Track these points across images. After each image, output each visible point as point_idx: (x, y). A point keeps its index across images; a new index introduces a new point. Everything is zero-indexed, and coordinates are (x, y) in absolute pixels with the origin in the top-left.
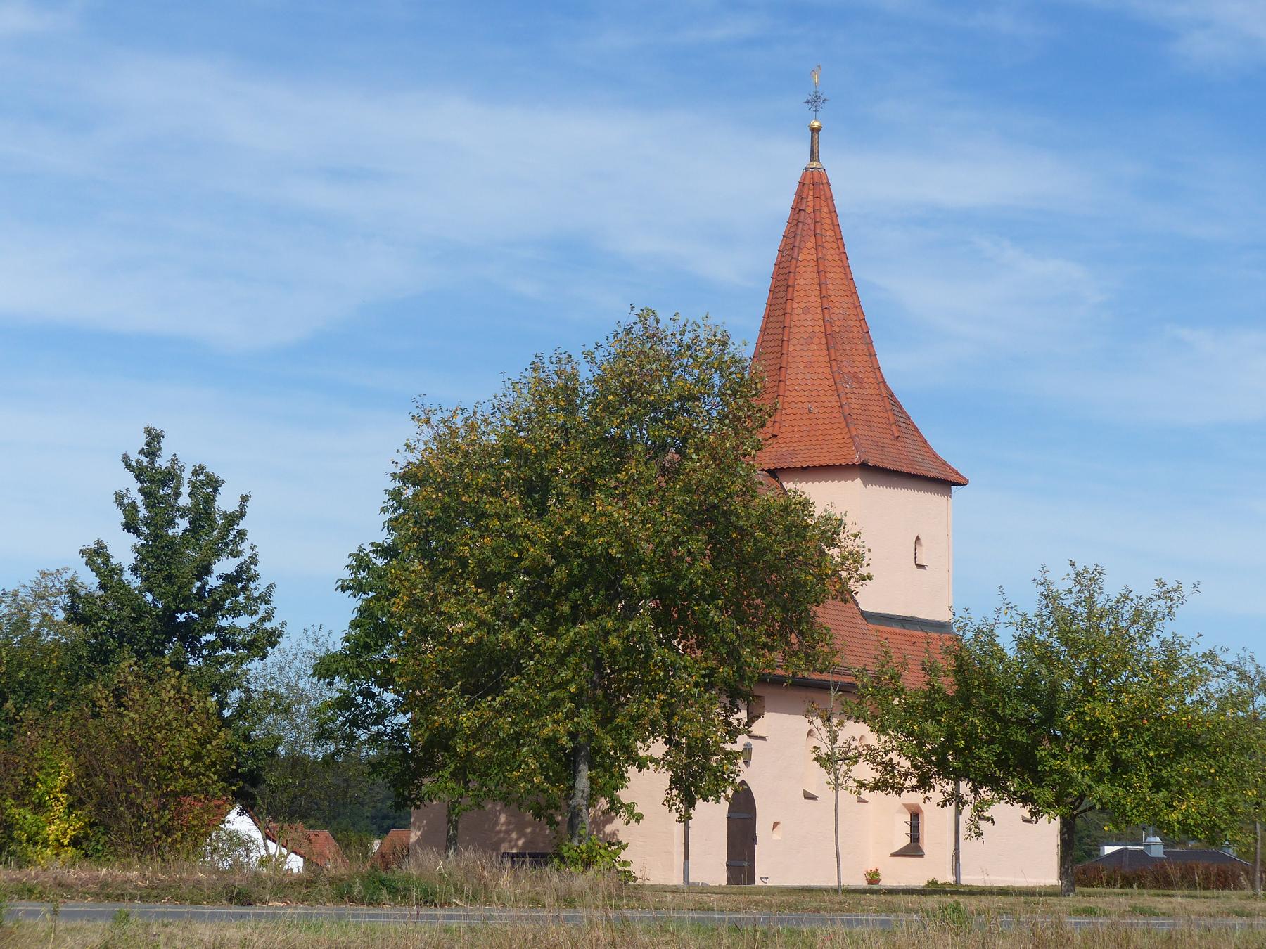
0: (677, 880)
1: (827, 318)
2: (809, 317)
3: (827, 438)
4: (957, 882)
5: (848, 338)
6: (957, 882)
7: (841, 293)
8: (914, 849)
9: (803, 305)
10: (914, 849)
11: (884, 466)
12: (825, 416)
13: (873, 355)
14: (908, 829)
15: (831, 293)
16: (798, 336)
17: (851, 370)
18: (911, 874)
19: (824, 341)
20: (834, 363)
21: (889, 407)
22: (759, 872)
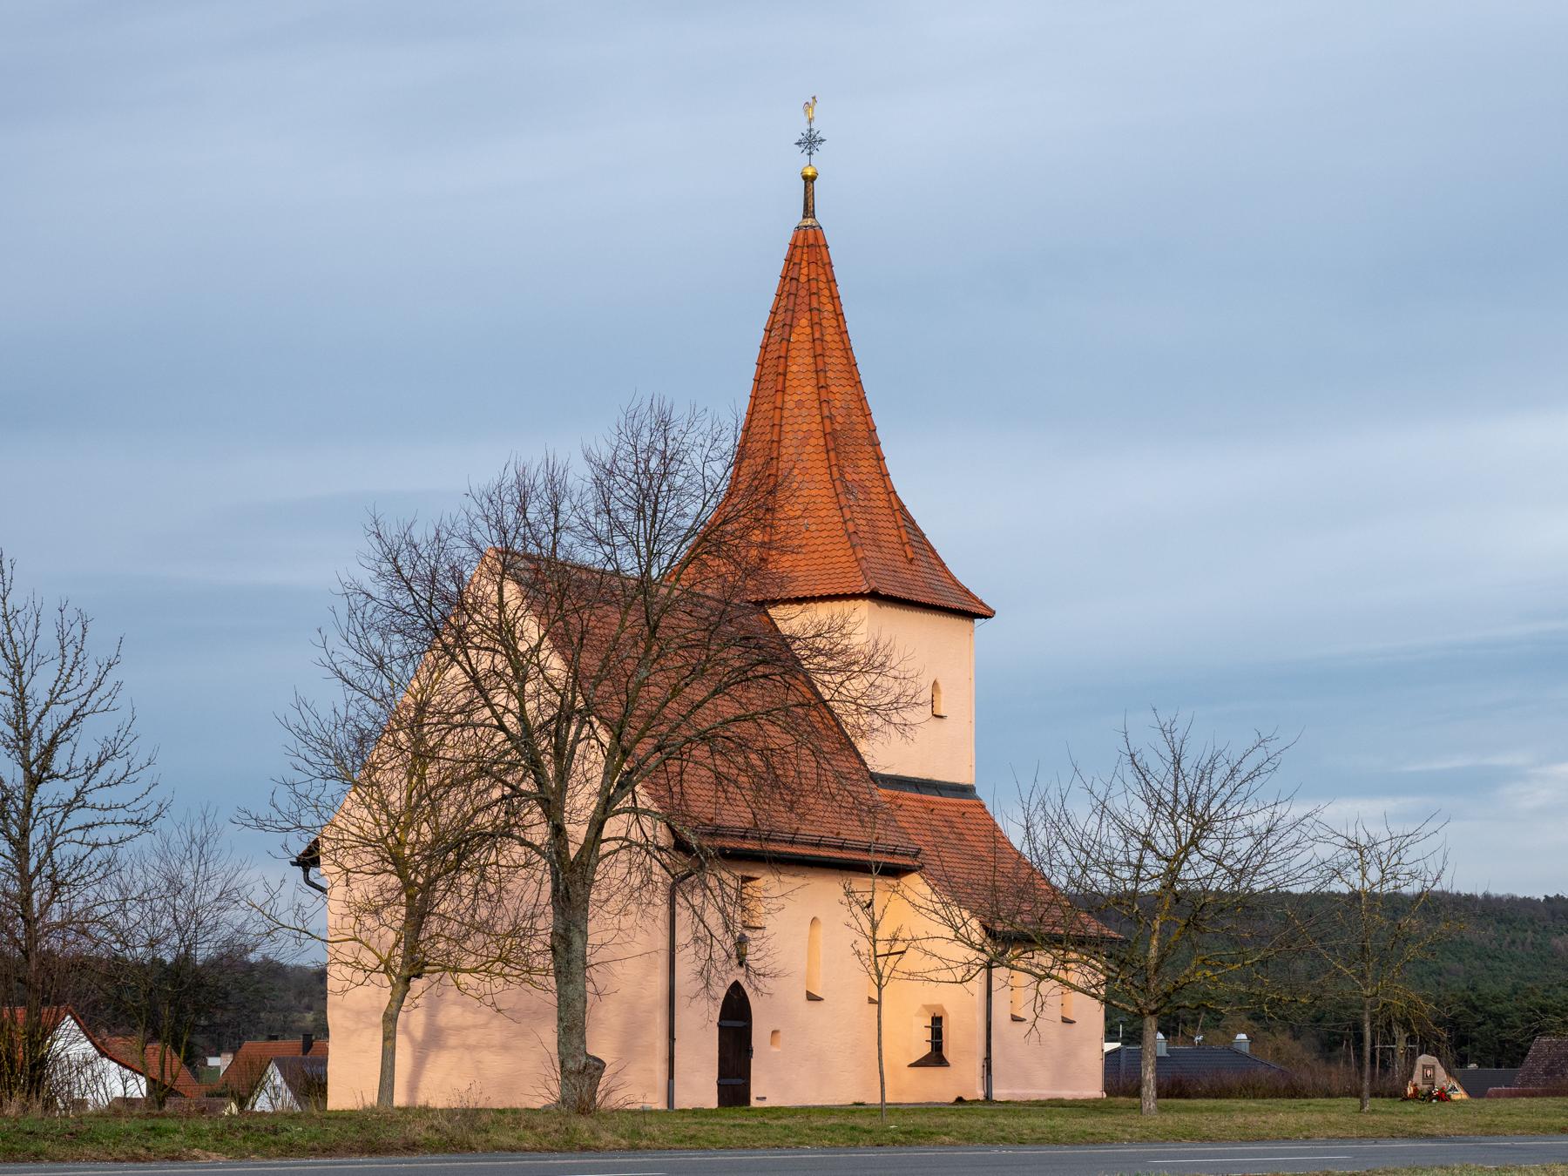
0: (660, 1105)
1: (826, 413)
2: (804, 412)
3: (827, 561)
4: (988, 1097)
5: (851, 440)
6: (988, 1097)
7: (843, 382)
8: (936, 1057)
9: (796, 398)
10: (936, 1057)
11: (898, 594)
12: (824, 534)
13: (880, 459)
14: (928, 1034)
15: (830, 382)
16: (790, 436)
17: (856, 477)
18: (938, 1087)
19: (822, 442)
20: (835, 469)
21: (901, 523)
22: (755, 1091)
